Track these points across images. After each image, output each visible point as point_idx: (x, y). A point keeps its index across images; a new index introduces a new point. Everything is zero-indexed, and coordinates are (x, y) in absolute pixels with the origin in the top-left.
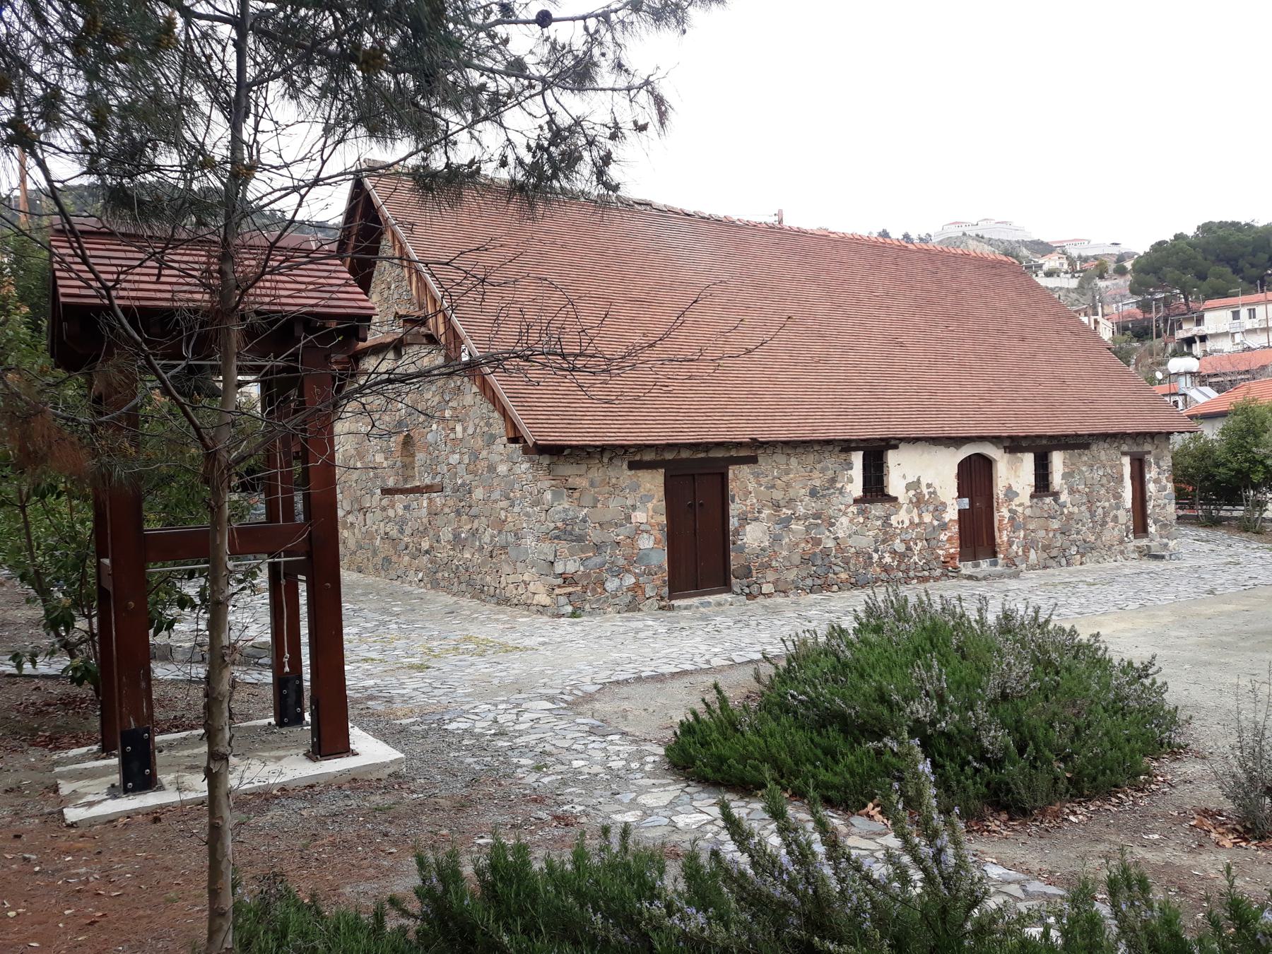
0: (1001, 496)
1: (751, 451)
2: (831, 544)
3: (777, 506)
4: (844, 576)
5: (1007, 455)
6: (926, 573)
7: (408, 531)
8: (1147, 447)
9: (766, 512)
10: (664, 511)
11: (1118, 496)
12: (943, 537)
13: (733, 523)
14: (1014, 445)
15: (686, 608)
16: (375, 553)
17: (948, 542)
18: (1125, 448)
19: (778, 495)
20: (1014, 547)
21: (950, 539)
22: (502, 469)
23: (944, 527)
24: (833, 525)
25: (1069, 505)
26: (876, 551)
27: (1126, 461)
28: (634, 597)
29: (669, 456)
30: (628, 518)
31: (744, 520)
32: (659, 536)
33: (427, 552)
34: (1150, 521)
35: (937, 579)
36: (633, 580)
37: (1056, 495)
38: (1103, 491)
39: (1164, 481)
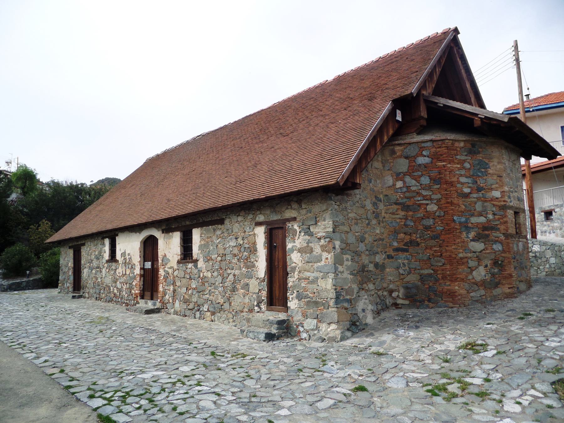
8: (289, 214)
11: (251, 266)
18: (261, 218)
20: (167, 297)
21: (136, 284)
38: (235, 261)
39: (317, 250)
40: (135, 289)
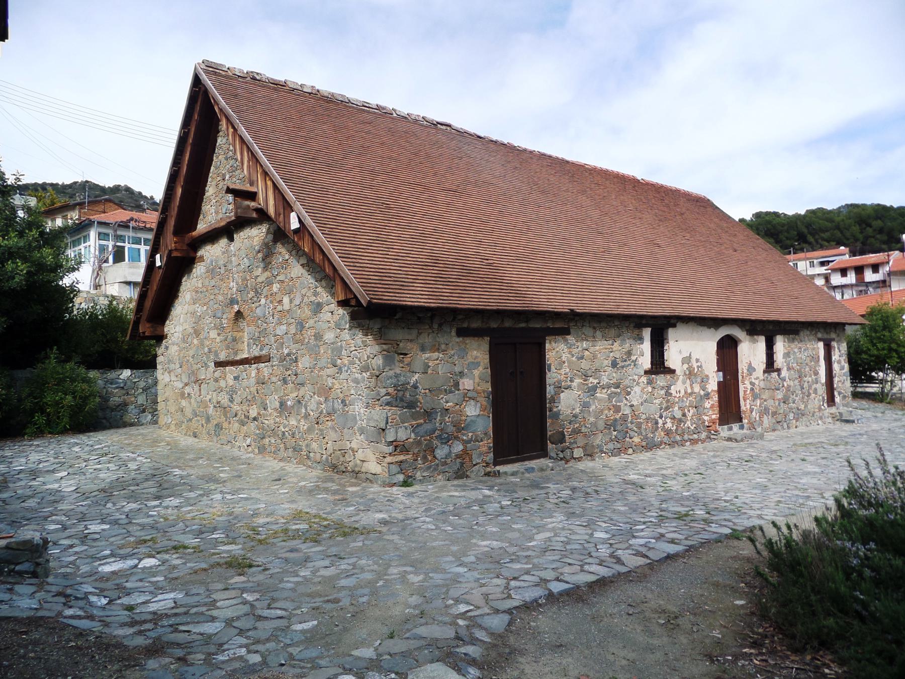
0: (745, 371)
1: (567, 322)
2: (627, 411)
3: (586, 376)
4: (637, 440)
5: (748, 337)
6: (695, 436)
7: (237, 399)
9: (578, 381)
10: (489, 379)
12: (707, 405)
13: (550, 390)
14: (754, 327)
15: (514, 474)
16: (208, 420)
17: (711, 410)
18: (820, 335)
19: (585, 365)
20: (754, 413)
21: (712, 406)
22: (329, 336)
23: (707, 396)
24: (629, 393)
25: (787, 379)
26: (661, 417)
27: (821, 345)
28: (462, 464)
29: (494, 325)
30: (456, 385)
31: (559, 388)
32: (485, 403)
33: (255, 419)
34: (836, 393)
35: (703, 441)
36: (461, 447)
37: (778, 371)
38: (807, 369)
39: (843, 363)
40: (711, 412)
